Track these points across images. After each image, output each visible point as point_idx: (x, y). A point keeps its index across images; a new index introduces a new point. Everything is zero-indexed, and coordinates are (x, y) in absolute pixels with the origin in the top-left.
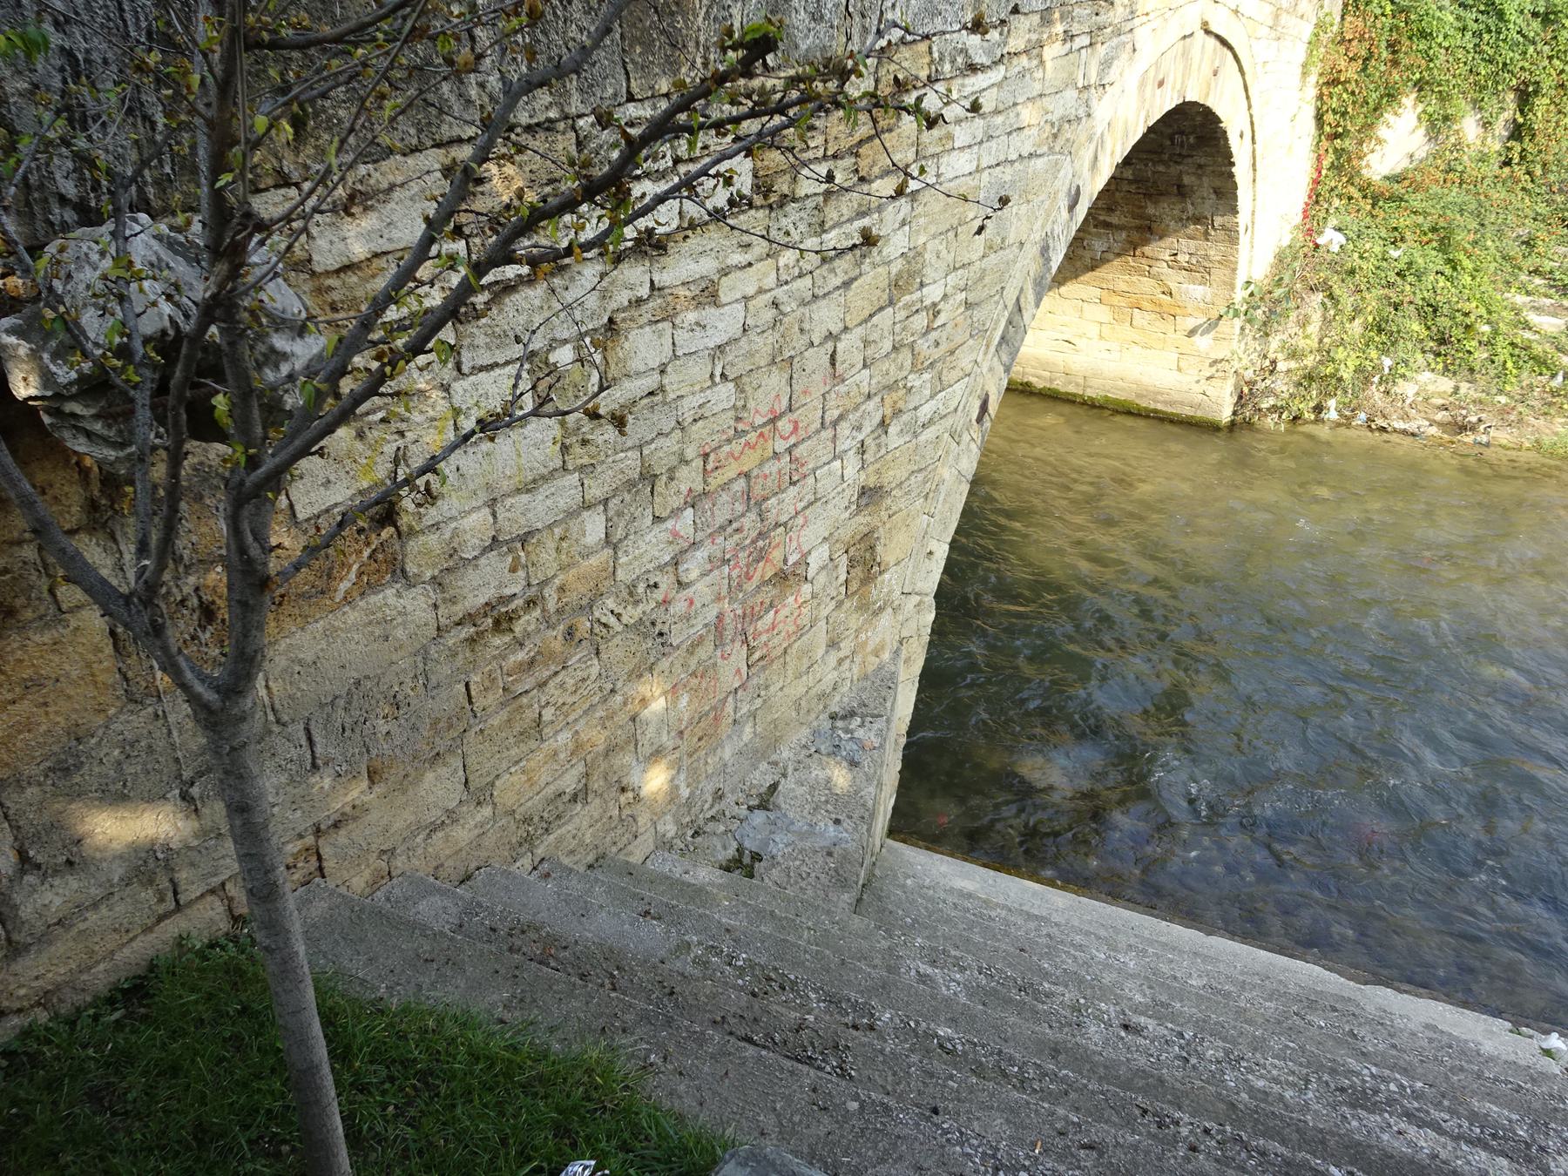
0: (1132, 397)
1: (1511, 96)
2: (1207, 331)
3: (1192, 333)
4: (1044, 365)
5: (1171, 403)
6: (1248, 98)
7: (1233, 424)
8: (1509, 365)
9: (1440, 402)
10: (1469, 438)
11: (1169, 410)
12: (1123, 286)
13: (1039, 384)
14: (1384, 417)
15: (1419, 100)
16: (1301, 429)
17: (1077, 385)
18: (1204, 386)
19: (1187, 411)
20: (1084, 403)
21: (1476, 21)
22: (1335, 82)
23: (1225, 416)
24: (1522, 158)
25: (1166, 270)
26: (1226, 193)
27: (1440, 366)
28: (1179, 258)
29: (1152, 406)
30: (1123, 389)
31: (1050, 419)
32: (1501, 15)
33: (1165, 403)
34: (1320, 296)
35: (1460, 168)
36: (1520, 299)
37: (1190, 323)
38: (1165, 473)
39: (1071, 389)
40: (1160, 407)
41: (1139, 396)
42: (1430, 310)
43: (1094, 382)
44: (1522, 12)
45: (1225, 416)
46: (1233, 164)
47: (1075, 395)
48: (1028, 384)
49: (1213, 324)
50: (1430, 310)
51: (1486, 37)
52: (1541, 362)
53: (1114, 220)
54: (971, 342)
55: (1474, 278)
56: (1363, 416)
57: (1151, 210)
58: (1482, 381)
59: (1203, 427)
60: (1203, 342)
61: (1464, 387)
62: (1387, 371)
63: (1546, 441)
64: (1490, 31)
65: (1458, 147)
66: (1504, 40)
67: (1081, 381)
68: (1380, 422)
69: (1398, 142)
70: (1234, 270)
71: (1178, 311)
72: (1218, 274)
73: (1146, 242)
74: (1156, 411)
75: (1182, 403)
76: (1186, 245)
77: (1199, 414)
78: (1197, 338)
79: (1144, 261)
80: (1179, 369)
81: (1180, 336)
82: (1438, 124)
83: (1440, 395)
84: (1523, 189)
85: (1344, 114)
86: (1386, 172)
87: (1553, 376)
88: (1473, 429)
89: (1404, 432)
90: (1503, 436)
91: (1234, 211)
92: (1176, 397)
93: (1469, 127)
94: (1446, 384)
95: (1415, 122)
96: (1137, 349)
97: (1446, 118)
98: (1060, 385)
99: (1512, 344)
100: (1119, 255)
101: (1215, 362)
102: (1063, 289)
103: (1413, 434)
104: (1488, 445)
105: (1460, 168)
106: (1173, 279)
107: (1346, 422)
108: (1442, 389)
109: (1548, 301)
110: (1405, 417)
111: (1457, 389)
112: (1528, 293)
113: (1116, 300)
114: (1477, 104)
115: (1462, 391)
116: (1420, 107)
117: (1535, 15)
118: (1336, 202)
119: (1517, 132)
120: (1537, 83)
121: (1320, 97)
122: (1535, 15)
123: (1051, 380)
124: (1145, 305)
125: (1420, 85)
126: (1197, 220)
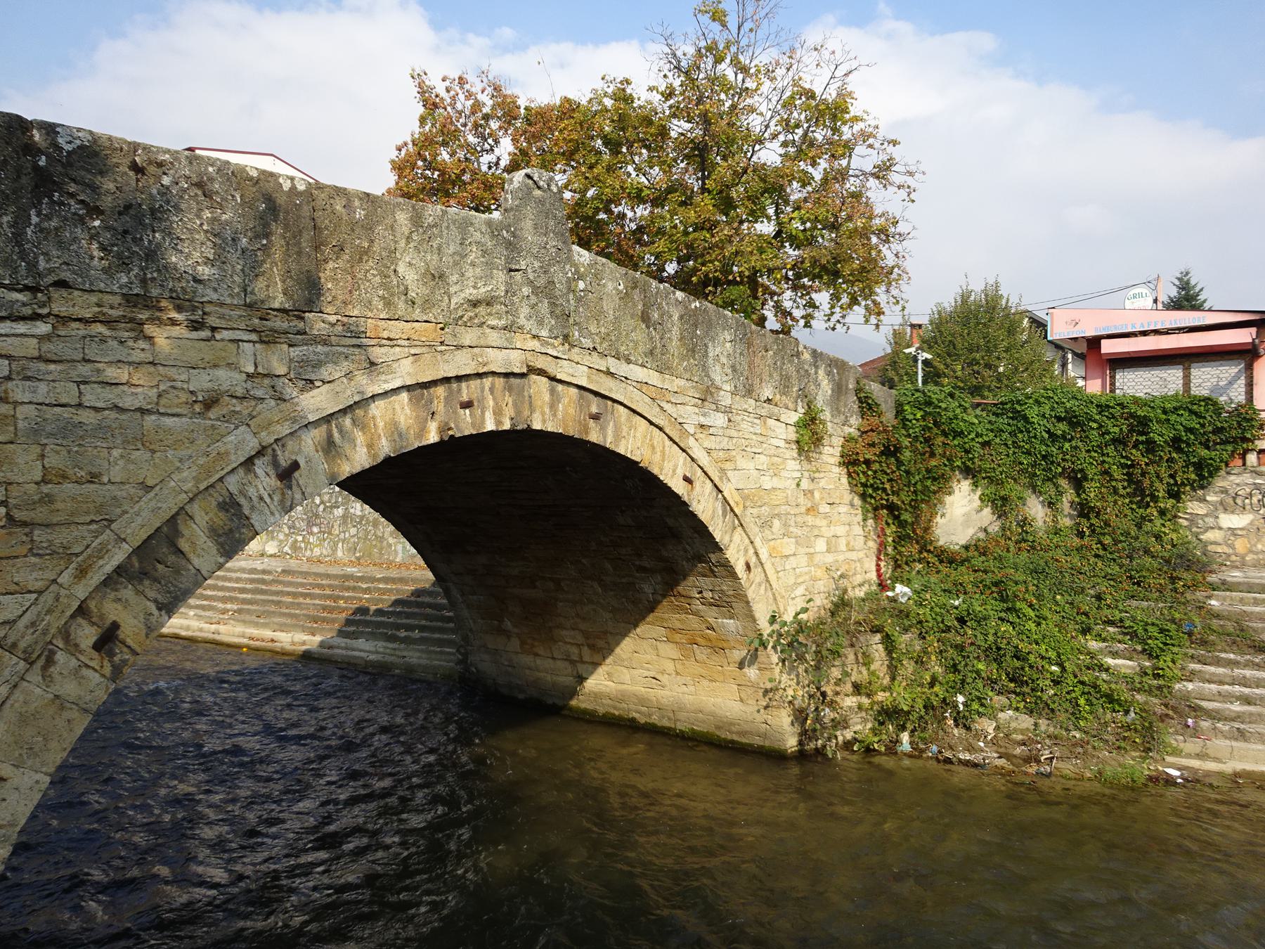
0: (712, 729)
1: (1063, 483)
2: (751, 663)
3: (741, 665)
4: (642, 701)
5: (743, 733)
6: (684, 451)
7: (802, 756)
8: (1082, 701)
9: (1020, 737)
10: (1032, 769)
11: (744, 740)
12: (678, 625)
13: (642, 720)
14: (951, 748)
15: (975, 485)
16: (872, 760)
17: (669, 719)
18: (763, 715)
19: (757, 741)
20: (677, 735)
21: (1009, 424)
22: (855, 463)
23: (791, 743)
24: (1093, 531)
25: (701, 607)
26: (701, 530)
27: (1021, 705)
28: (705, 594)
29: (729, 737)
30: (704, 722)
31: (637, 749)
32: (1025, 418)
33: (739, 733)
34: (878, 637)
35: (1031, 538)
36: (1094, 645)
37: (739, 654)
38: (701, 792)
39: (665, 723)
40: (736, 738)
41: (718, 728)
42: (995, 654)
43: (682, 715)
44: (1044, 416)
45: (791, 743)
46: (685, 504)
47: (669, 729)
48: (633, 720)
49: (753, 657)
50: (995, 654)
51: (1020, 436)
52: (1110, 698)
53: (646, 564)
54: (33, 559)
55: (1039, 624)
56: (935, 748)
57: (665, 554)
58: (1063, 717)
59: (775, 757)
60: (752, 672)
61: (1043, 723)
62: (961, 707)
63: (1109, 772)
64: (1021, 432)
65: (1024, 522)
66: (1035, 437)
67: (671, 715)
68: (948, 754)
69: (961, 514)
70: (748, 602)
71: (725, 645)
72: (738, 606)
73: (678, 584)
74: (733, 742)
75: (751, 733)
76: (705, 582)
77: (767, 744)
78: (746, 670)
79: (682, 599)
80: (742, 700)
81: (733, 668)
82: (1001, 505)
83: (1022, 732)
84: (1097, 556)
85: (884, 490)
86: (963, 542)
87: (1127, 712)
88: (1038, 762)
89: (966, 763)
90: (1068, 768)
91: (717, 548)
92: (746, 727)
93: (1036, 510)
94: (1026, 722)
95: (979, 502)
96: (705, 683)
97: (1004, 499)
98: (655, 719)
99: (1082, 683)
100: (664, 596)
101: (766, 692)
102: (638, 630)
103: (976, 765)
104: (1049, 775)
105: (1031, 538)
106: (711, 615)
107: (917, 753)
108: (1024, 726)
109: (1122, 646)
110: (971, 749)
111: (1036, 724)
112: (1104, 640)
113: (677, 637)
114: (1034, 488)
115: (1043, 728)
116: (979, 493)
117: (1059, 419)
118: (919, 566)
119: (1084, 510)
120: (1082, 470)
121: (849, 475)
122: (1059, 419)
123: (650, 715)
124: (699, 640)
125: (968, 472)
126: (701, 558)
